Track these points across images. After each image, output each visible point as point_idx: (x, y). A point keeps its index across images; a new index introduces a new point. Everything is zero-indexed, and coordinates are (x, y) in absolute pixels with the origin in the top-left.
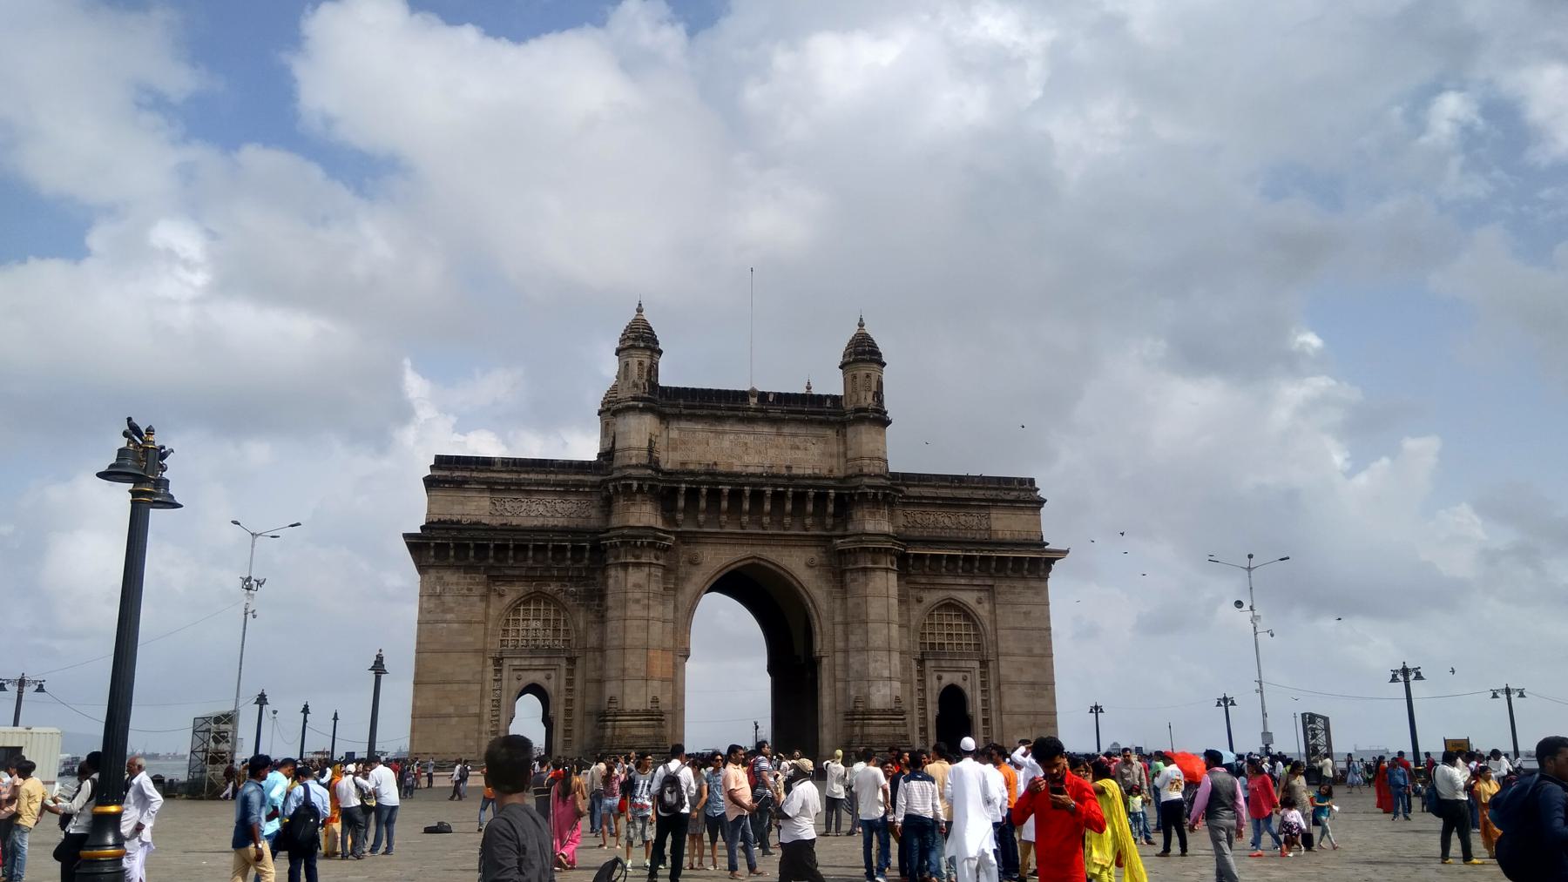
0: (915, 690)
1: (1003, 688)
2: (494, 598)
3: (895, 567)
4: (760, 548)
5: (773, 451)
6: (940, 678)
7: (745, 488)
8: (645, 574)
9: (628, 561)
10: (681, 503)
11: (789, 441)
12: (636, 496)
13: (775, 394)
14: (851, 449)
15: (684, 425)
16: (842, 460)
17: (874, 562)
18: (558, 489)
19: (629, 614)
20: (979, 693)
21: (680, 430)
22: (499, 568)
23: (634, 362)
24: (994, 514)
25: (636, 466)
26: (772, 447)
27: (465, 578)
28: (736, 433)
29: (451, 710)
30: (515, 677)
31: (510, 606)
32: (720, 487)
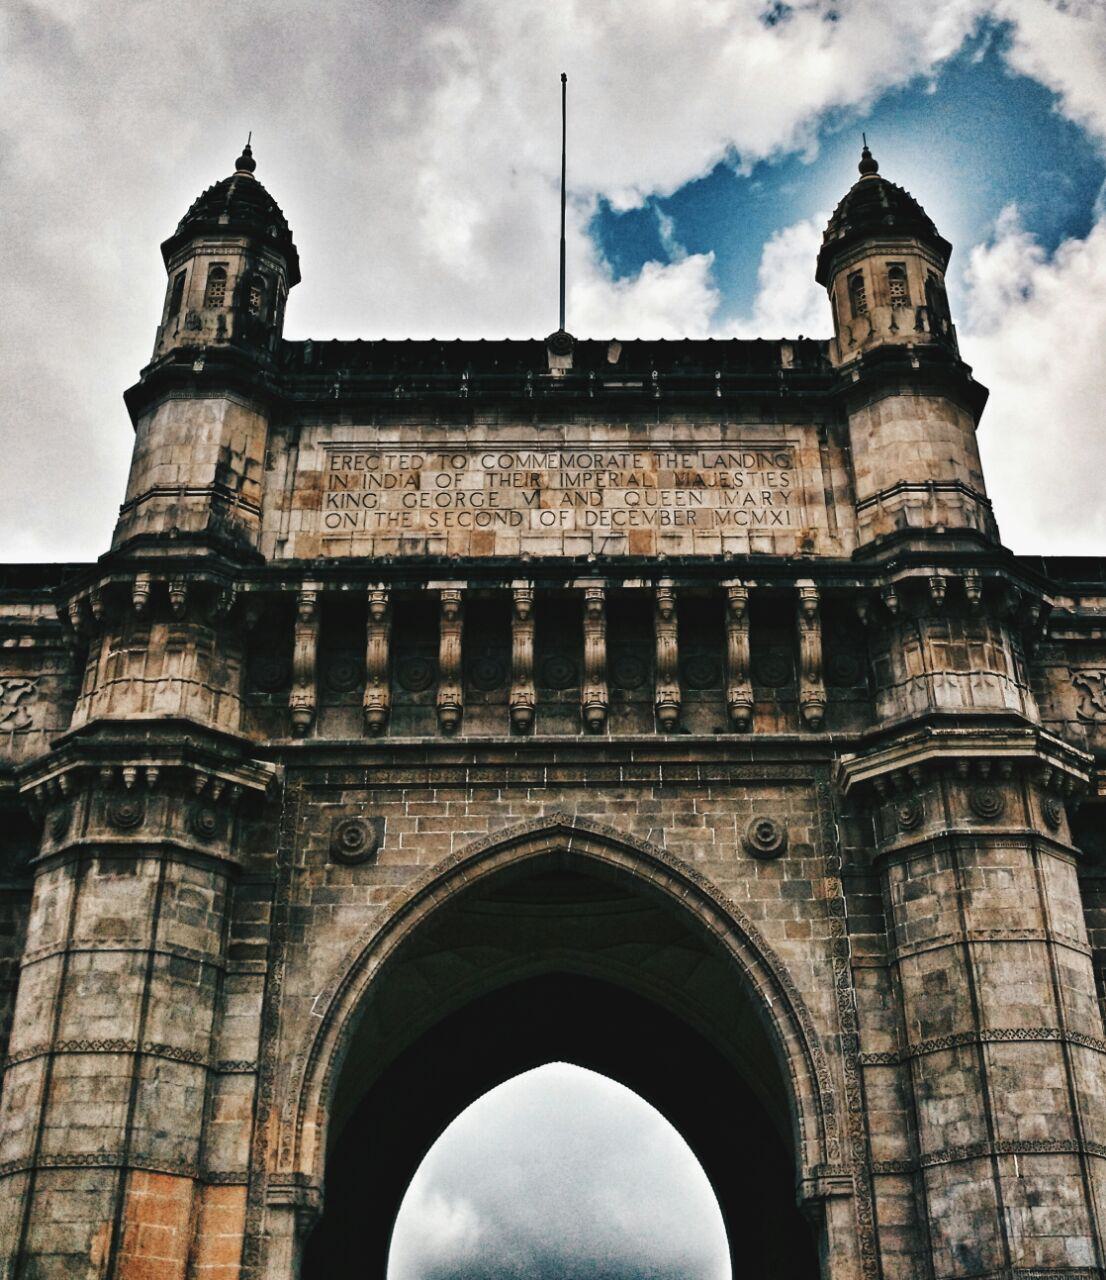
3: (1064, 837)
4: (580, 797)
5: (624, 493)
7: (516, 584)
8: (146, 882)
9: (89, 839)
11: (671, 463)
12: (149, 631)
13: (626, 345)
14: (865, 473)
15: (343, 434)
16: (843, 512)
19: (70, 1031)
21: (331, 448)
23: (198, 270)
25: (160, 540)
26: (615, 482)
28: (508, 449)
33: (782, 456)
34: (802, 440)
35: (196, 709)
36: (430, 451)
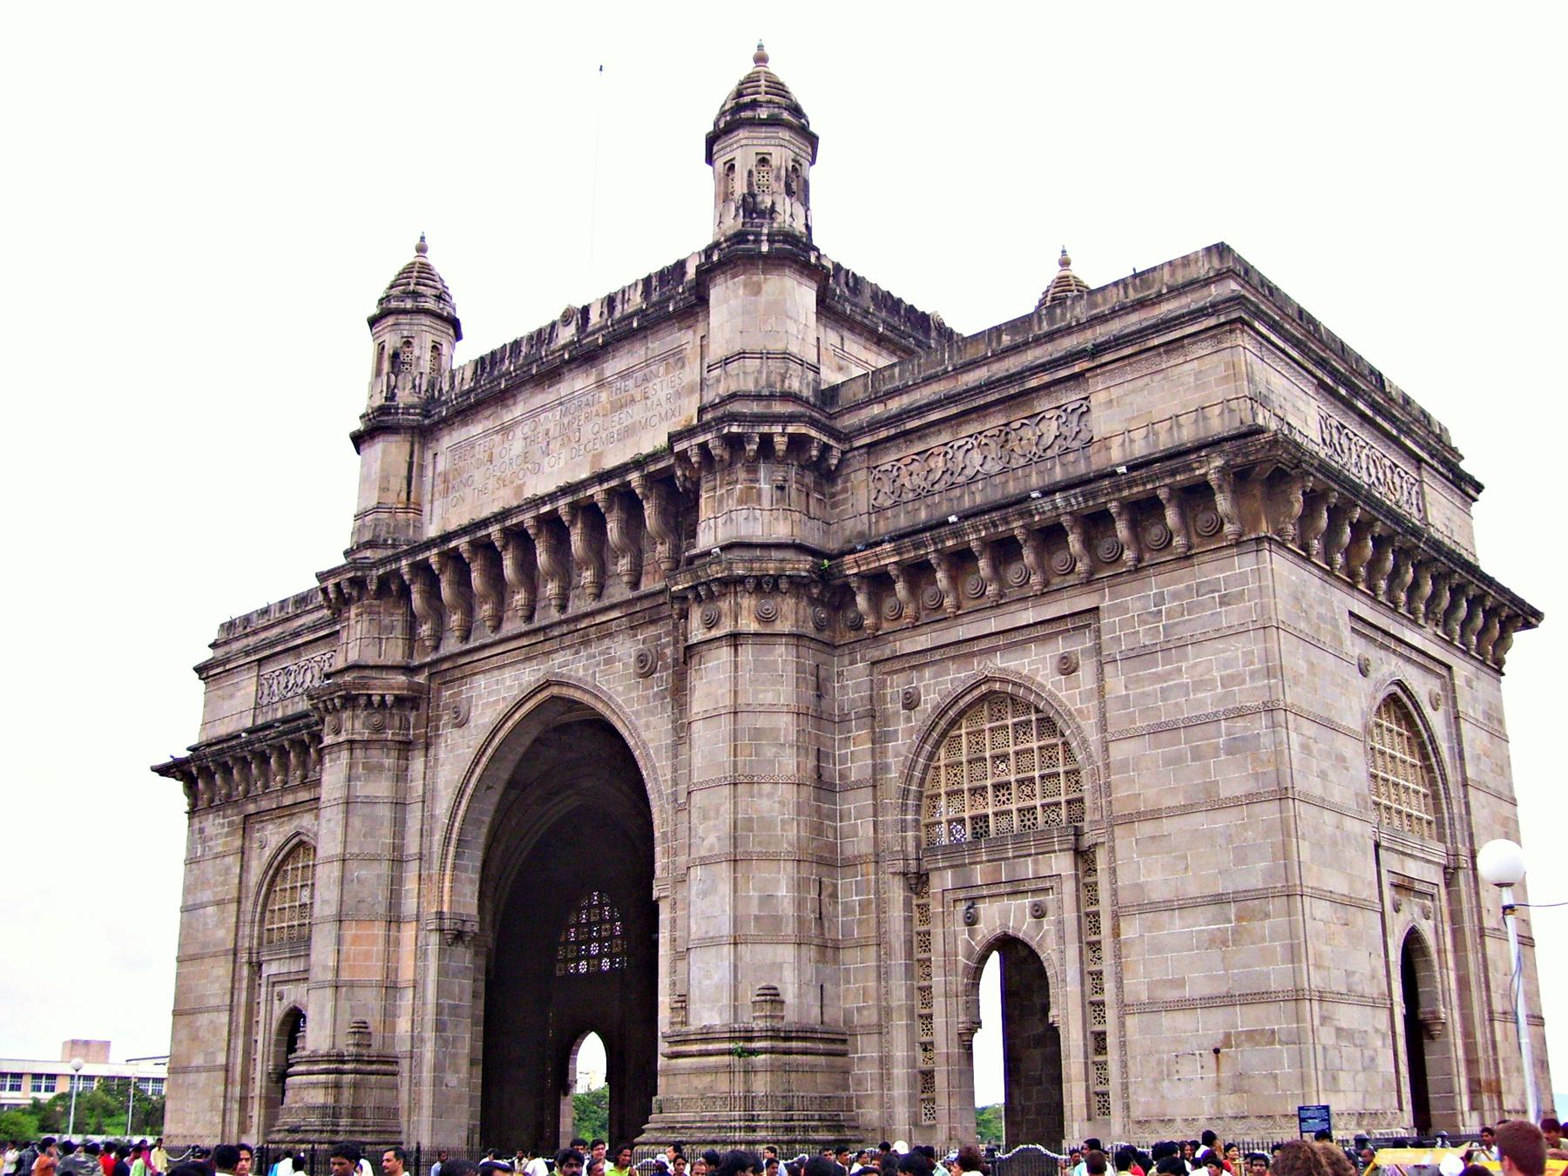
0: (898, 961)
1: (1130, 930)
2: (255, 853)
6: (971, 921)
7: (490, 530)
10: (417, 600)
15: (460, 435)
17: (711, 624)
18: (322, 633)
20: (1072, 951)
22: (255, 799)
24: (1100, 392)
27: (223, 825)
28: (533, 414)
29: (198, 1060)
30: (276, 998)
31: (270, 865)
32: (453, 544)
33: (676, 357)
34: (686, 338)
35: (371, 658)
36: (497, 432)
